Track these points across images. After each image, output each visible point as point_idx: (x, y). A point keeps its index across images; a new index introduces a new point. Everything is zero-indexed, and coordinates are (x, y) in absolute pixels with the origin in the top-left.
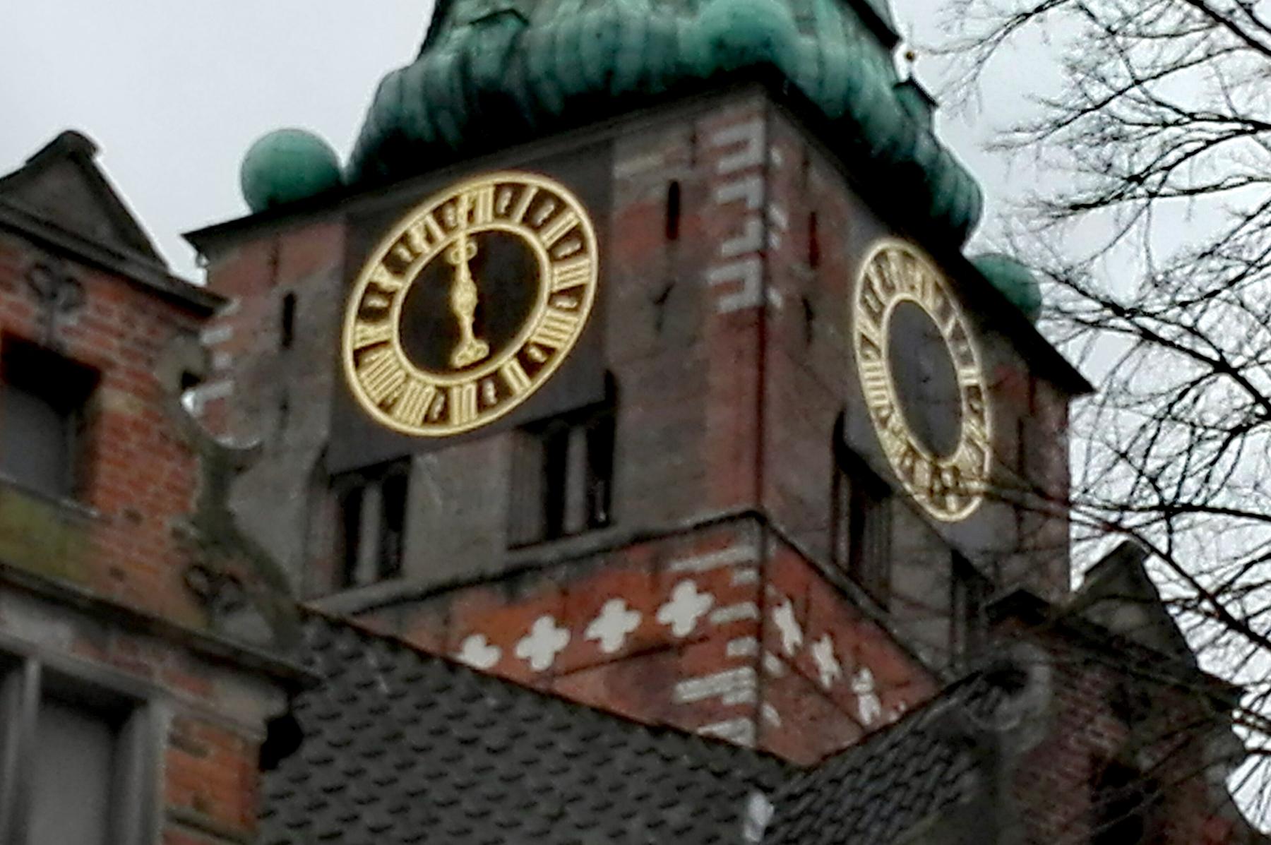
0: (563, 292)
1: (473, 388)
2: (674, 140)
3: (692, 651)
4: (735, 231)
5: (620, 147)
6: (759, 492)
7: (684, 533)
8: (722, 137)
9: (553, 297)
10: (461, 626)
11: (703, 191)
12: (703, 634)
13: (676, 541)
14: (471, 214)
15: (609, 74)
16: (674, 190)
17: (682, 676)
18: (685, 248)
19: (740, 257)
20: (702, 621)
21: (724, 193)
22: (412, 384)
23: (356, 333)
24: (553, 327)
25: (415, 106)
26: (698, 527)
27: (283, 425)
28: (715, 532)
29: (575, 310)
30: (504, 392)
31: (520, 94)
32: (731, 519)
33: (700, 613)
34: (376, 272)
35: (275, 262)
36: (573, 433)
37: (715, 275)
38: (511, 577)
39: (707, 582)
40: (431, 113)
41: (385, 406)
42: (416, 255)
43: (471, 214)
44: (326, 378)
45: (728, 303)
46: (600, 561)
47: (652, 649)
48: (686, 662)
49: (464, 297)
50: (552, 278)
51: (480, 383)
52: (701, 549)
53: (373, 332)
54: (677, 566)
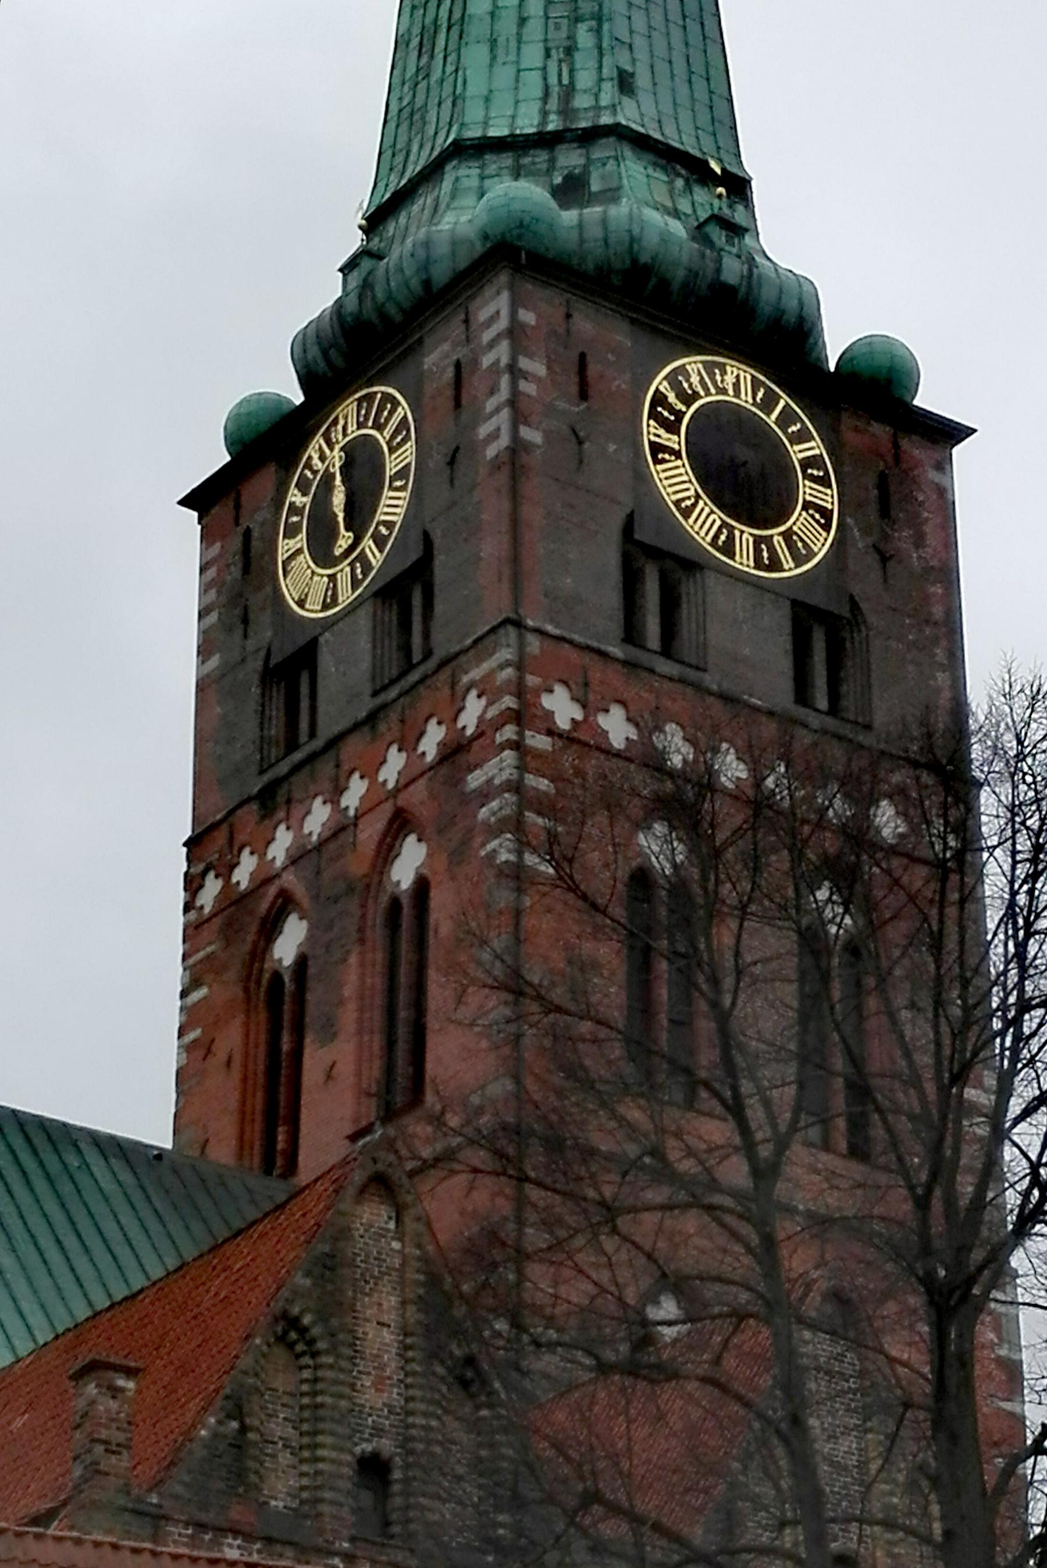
0: (731, 538)
1: (348, 569)
2: (456, 328)
3: (476, 746)
4: (492, 391)
5: (428, 342)
6: (516, 600)
7: (465, 651)
8: (483, 315)
9: (392, 479)
10: (346, 768)
11: (475, 362)
12: (485, 729)
13: (463, 659)
14: (345, 428)
15: (427, 283)
16: (458, 365)
17: (471, 769)
18: (465, 417)
19: (497, 410)
20: (481, 719)
21: (486, 361)
22: (316, 578)
23: (285, 547)
24: (393, 506)
25: (314, 352)
26: (476, 642)
27: (245, 636)
28: (487, 642)
29: (714, 542)
30: (367, 567)
31: (375, 318)
32: (493, 630)
33: (478, 714)
34: (295, 497)
35: (238, 507)
36: (405, 591)
37: (483, 431)
38: (372, 719)
39: (486, 689)
40: (325, 353)
41: (301, 603)
42: (315, 473)
43: (345, 428)
44: (268, 589)
45: (491, 452)
46: (421, 689)
47: (457, 752)
48: (471, 757)
49: (339, 499)
50: (745, 535)
51: (352, 564)
52: (479, 661)
53: (294, 544)
54: (465, 679)
